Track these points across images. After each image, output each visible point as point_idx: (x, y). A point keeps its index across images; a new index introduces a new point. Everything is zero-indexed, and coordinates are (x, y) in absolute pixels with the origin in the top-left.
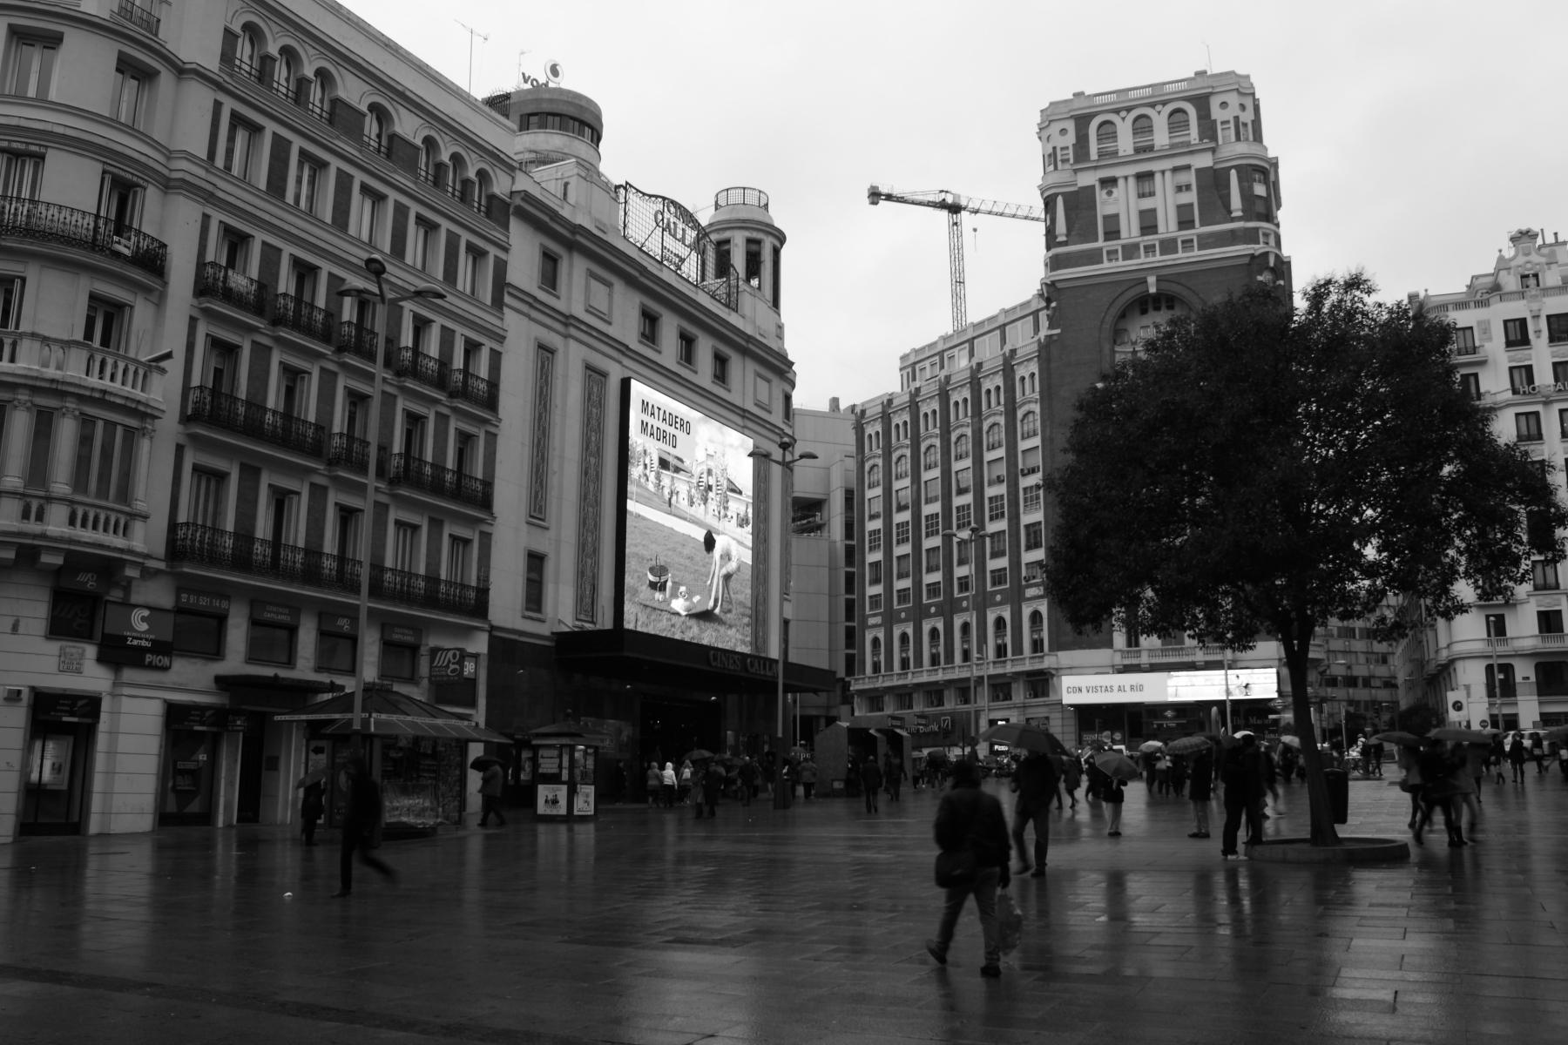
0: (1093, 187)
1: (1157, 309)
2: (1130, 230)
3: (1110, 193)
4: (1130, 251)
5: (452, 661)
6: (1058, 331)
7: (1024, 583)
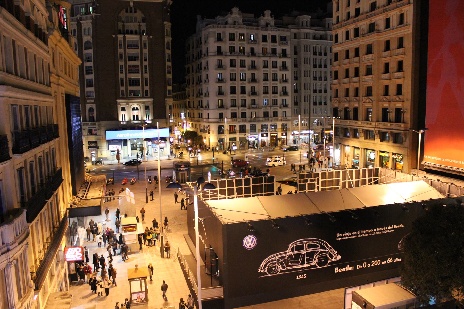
5: (77, 252)
6: (100, 15)
7: (86, 98)
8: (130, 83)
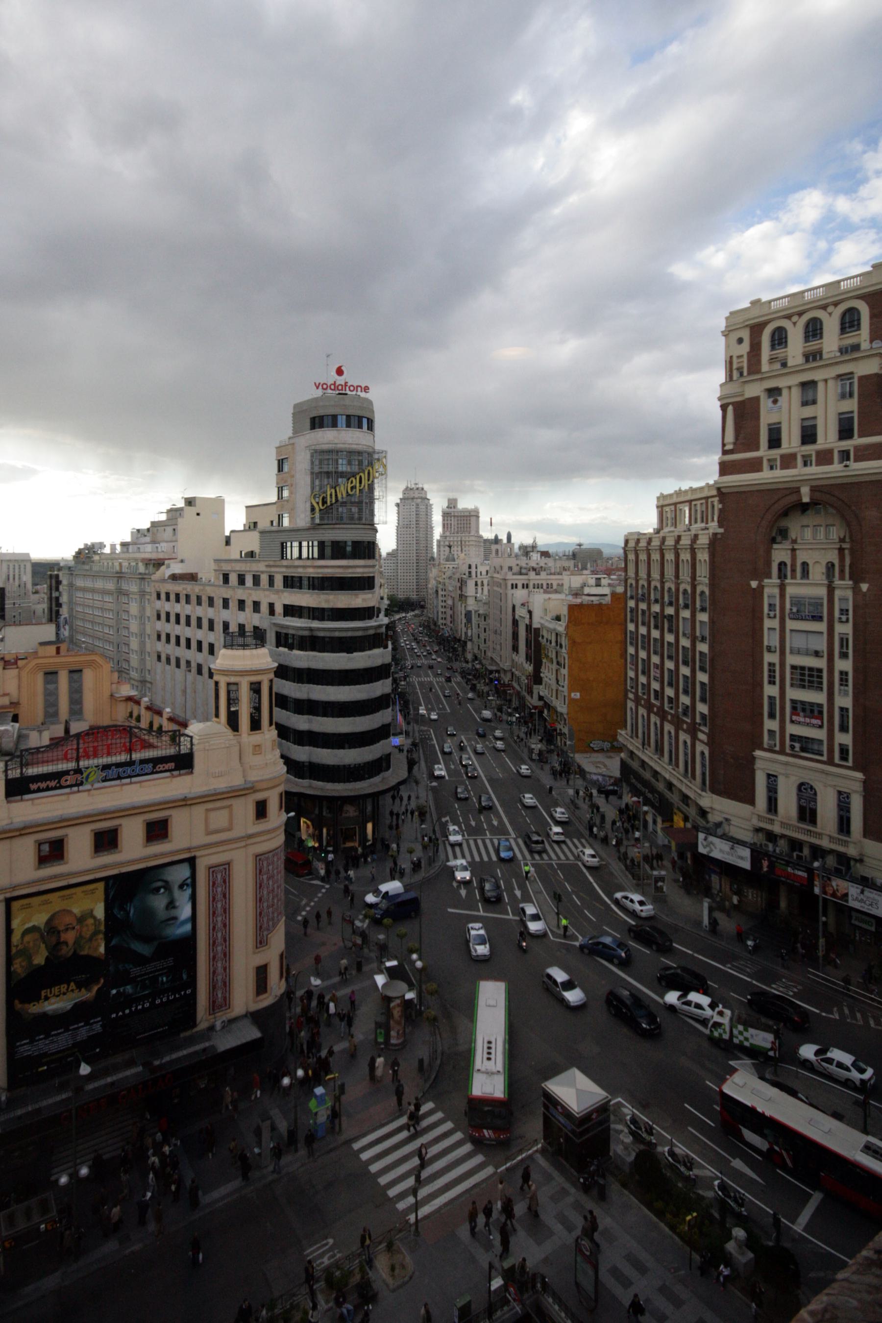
0: (757, 399)
2: (791, 441)
3: (775, 402)
4: (788, 461)
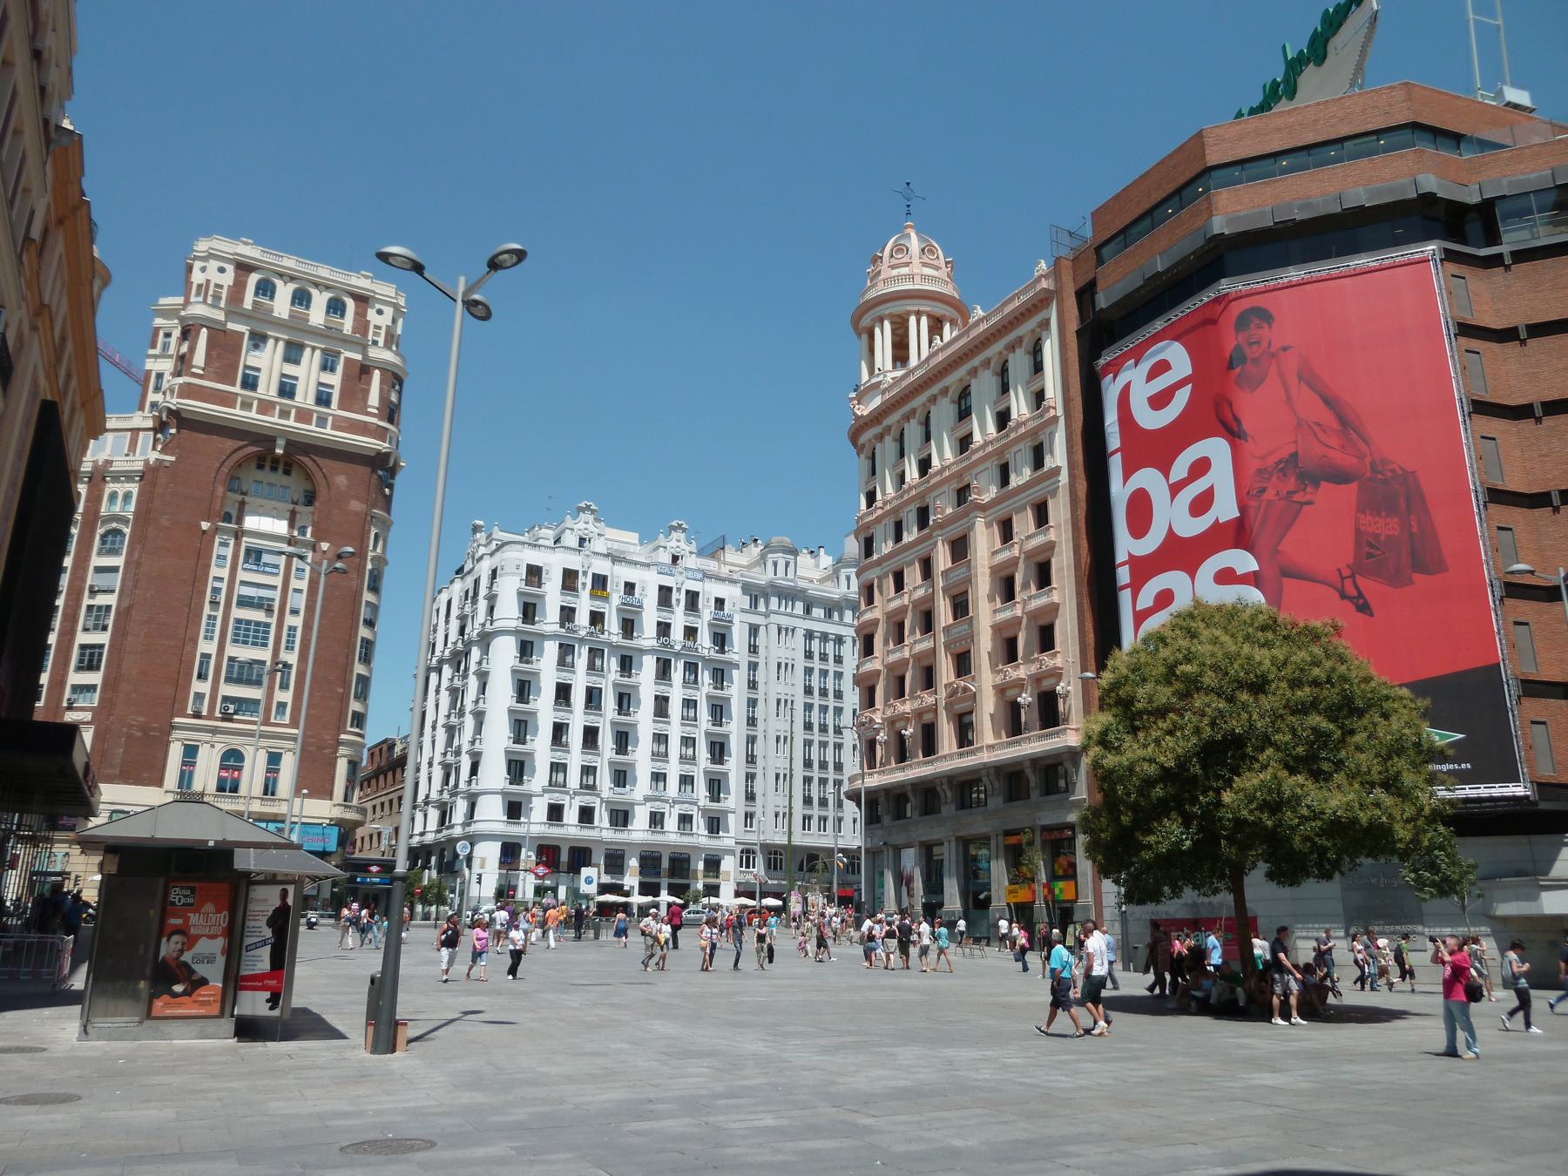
0: (242, 334)
1: (274, 469)
2: (267, 389)
4: (266, 407)
6: (173, 459)
8: (228, 672)
